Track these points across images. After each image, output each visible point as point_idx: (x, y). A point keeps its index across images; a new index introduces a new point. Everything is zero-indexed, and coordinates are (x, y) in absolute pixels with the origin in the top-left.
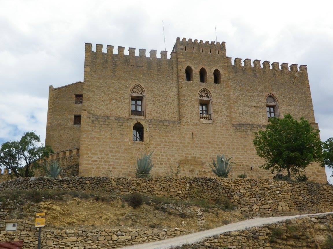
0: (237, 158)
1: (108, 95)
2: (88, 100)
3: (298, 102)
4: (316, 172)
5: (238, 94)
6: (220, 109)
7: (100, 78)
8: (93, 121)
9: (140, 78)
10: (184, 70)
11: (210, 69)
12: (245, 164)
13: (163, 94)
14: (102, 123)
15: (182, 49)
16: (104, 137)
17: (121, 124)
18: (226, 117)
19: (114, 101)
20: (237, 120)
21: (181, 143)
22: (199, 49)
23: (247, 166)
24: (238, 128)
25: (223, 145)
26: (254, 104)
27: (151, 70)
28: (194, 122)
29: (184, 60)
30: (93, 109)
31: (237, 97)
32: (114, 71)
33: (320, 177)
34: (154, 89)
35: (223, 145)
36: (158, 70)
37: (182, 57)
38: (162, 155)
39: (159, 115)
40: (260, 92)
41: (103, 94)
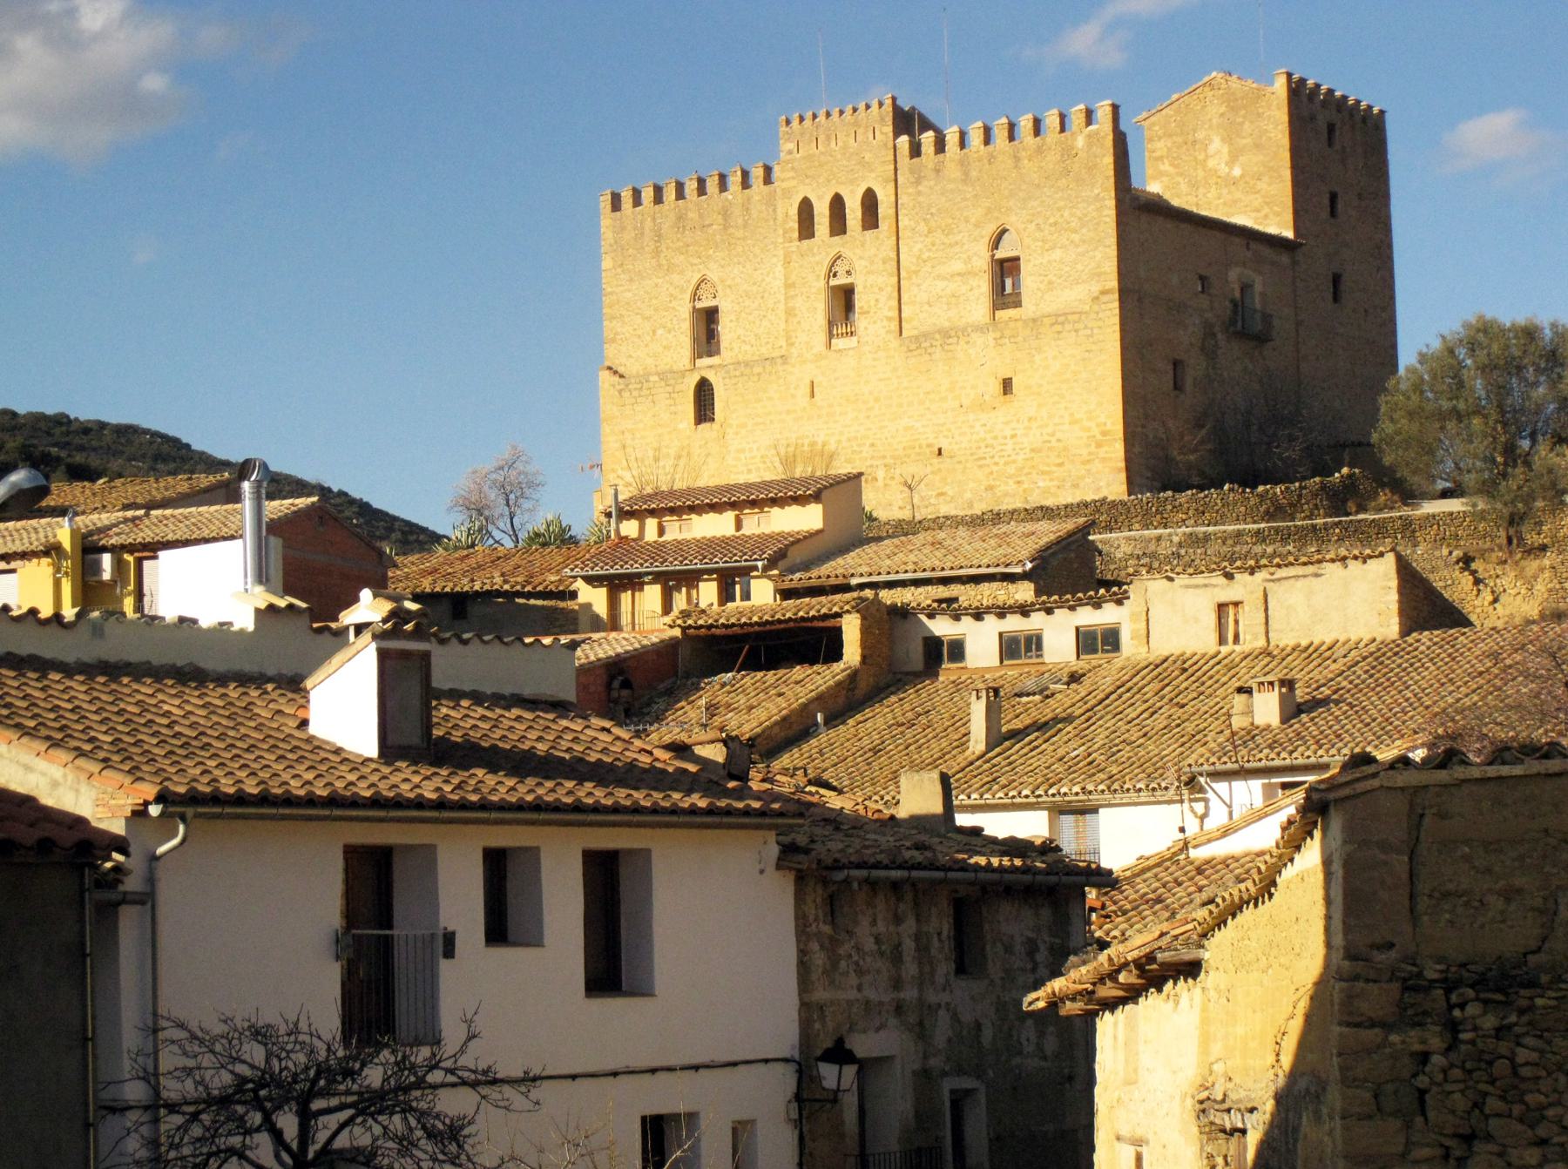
0: (907, 429)
1: (648, 318)
2: (613, 341)
3: (1075, 231)
4: (1099, 437)
5: (919, 246)
6: (873, 303)
7: (631, 280)
8: (620, 392)
9: (709, 257)
10: (794, 211)
11: (852, 192)
12: (924, 443)
13: (755, 288)
14: (635, 393)
15: (790, 152)
16: (641, 426)
17: (669, 389)
18: (885, 323)
19: (660, 332)
20: (915, 323)
21: (788, 412)
22: (828, 138)
23: (929, 446)
24: (913, 347)
25: (877, 400)
26: (958, 266)
27: (731, 230)
28: (815, 351)
29: (793, 183)
30: (624, 360)
31: (919, 258)
32: (657, 253)
33: (1105, 448)
34: (738, 280)
35: (877, 400)
36: (745, 226)
37: (792, 174)
38: (751, 450)
39: (748, 348)
40: (977, 226)
41: (638, 320)
